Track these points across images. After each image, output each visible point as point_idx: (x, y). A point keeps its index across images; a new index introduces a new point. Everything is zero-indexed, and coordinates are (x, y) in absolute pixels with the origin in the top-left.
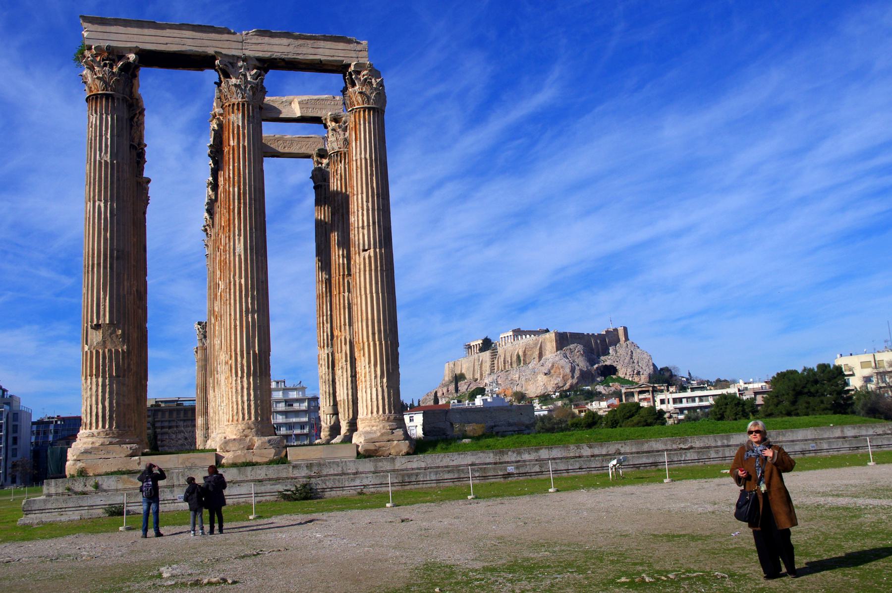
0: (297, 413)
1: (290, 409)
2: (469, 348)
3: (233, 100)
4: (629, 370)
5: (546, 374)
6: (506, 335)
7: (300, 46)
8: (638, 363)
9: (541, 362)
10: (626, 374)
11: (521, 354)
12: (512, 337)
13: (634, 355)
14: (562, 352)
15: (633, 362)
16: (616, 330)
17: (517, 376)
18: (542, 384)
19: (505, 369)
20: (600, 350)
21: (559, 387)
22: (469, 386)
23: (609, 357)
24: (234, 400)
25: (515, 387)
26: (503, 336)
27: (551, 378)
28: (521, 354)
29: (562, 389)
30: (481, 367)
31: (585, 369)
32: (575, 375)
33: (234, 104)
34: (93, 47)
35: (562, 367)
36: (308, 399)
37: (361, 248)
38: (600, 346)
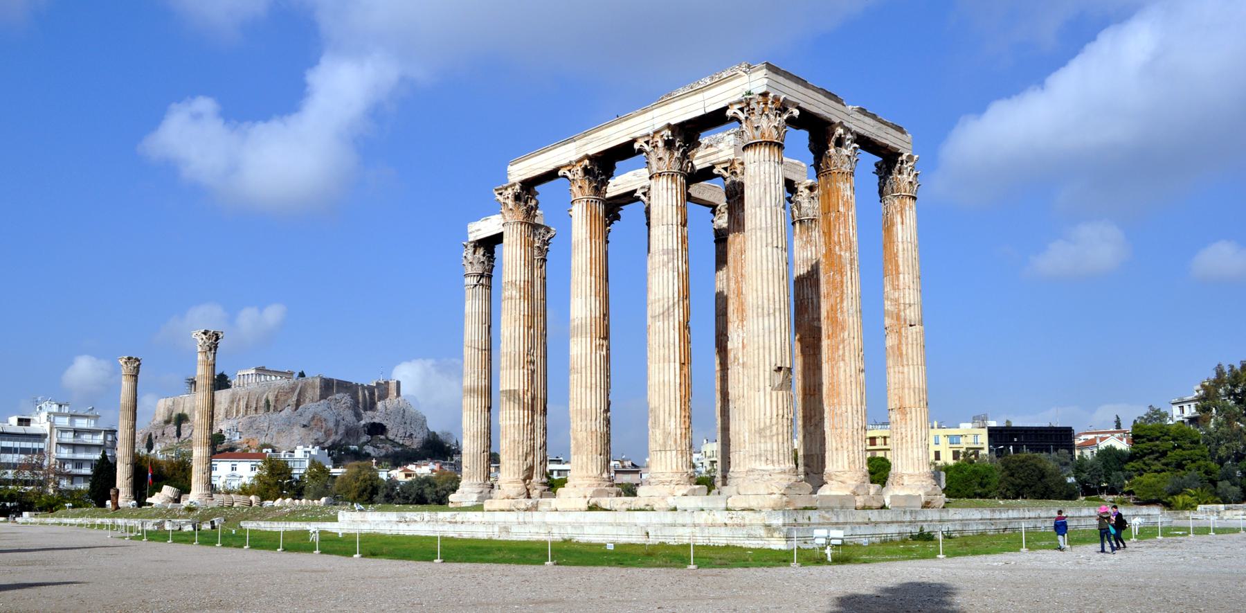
0: (88, 447)
1: (78, 441)
2: (192, 383)
3: (843, 169)
4: (401, 431)
5: (304, 426)
6: (246, 373)
7: (879, 129)
8: (411, 424)
10: (396, 436)
11: (271, 399)
12: (254, 376)
13: (406, 414)
15: (405, 423)
16: (387, 383)
17: (266, 424)
19: (246, 414)
24: (850, 448)
28: (271, 399)
32: (339, 431)
33: (843, 173)
34: (771, 95)
35: (325, 420)
36: (105, 431)
37: (908, 322)
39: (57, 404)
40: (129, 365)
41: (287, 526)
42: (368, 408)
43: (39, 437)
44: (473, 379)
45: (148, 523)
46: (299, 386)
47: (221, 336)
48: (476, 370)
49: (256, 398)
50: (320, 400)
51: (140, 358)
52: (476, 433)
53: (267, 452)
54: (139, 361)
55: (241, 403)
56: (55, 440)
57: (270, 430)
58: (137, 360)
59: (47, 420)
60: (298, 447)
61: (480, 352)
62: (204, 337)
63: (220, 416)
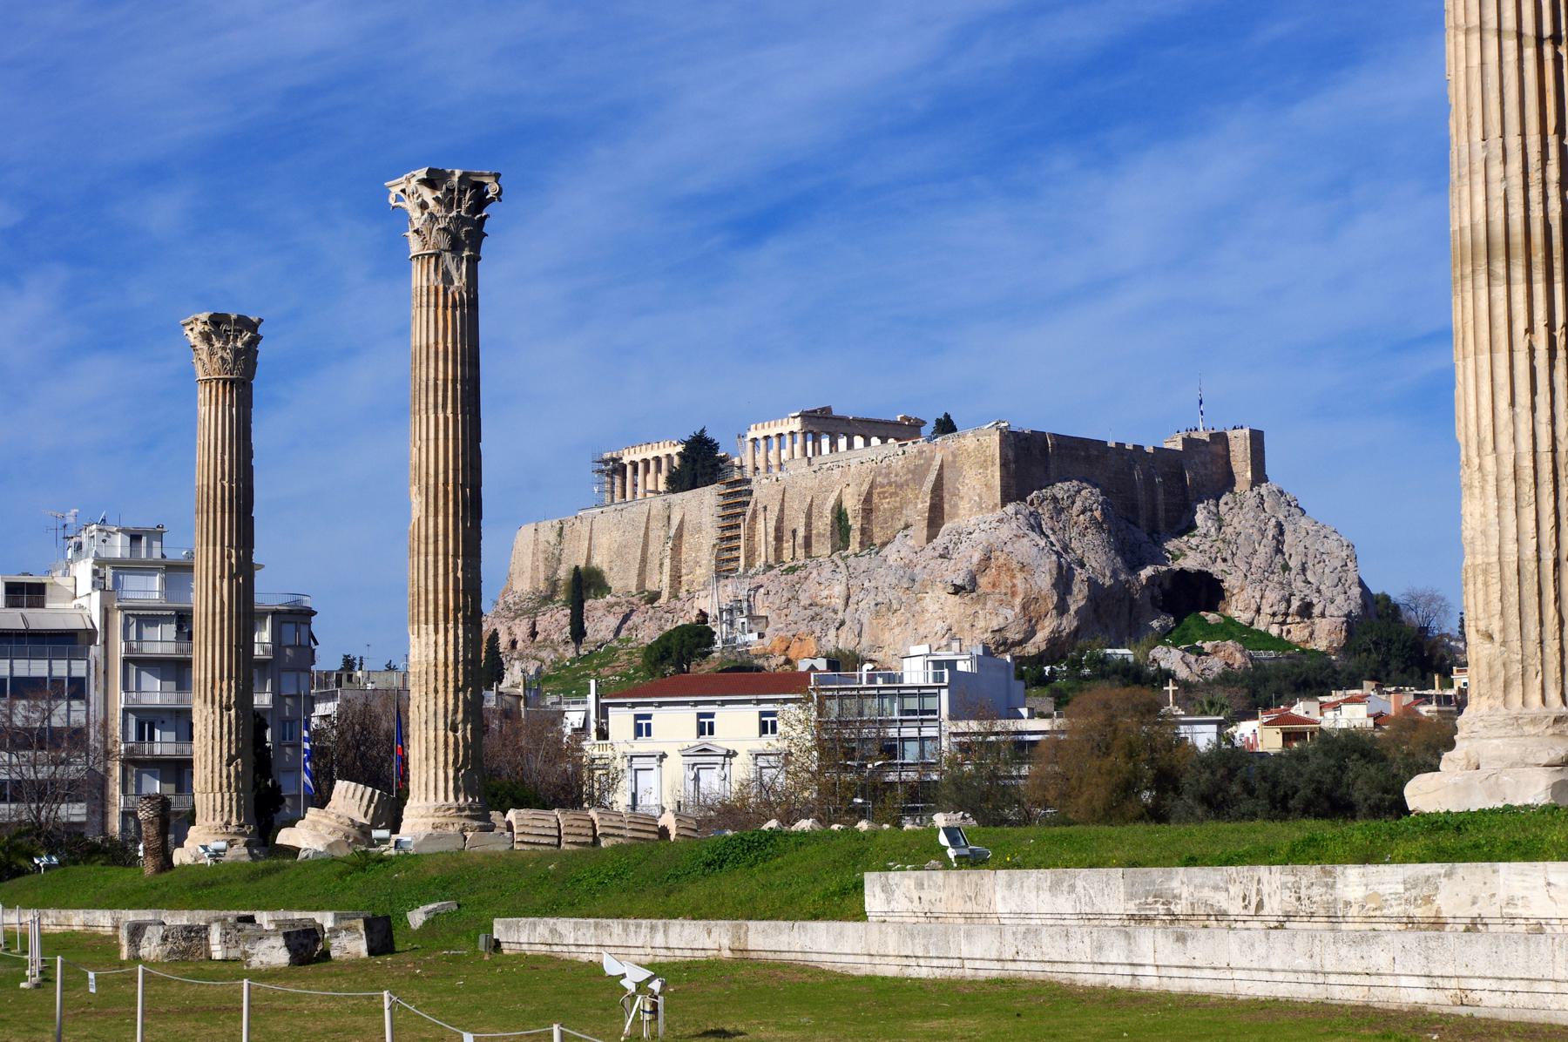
2: (614, 471)
4: (1273, 596)
5: (958, 590)
6: (773, 432)
9: (941, 540)
10: (1258, 611)
11: (851, 505)
12: (799, 438)
14: (1025, 509)
15: (1286, 568)
16: (1220, 439)
17: (838, 589)
18: (940, 626)
19: (779, 559)
20: (1161, 514)
21: (1006, 645)
22: (626, 618)
23: (1194, 541)
25: (832, 632)
26: (760, 434)
27: (978, 608)
28: (851, 505)
29: (1017, 651)
30: (676, 550)
31: (1108, 582)
32: (1070, 600)
35: (1023, 567)
36: (275, 613)
38: (1161, 497)
39: (124, 531)
40: (217, 345)
41: (659, 940)
42: (1162, 525)
43: (69, 641)
44: (1497, 191)
45: (150, 931)
46: (937, 463)
47: (492, 189)
48: (1514, 142)
49: (805, 506)
50: (1004, 505)
51: (255, 319)
52: (1527, 462)
53: (813, 668)
54: (253, 327)
55: (760, 526)
56: (119, 649)
57: (852, 607)
58: (244, 323)
59: (94, 584)
60: (914, 650)
61: (1530, 52)
62: (428, 195)
63: (698, 571)
